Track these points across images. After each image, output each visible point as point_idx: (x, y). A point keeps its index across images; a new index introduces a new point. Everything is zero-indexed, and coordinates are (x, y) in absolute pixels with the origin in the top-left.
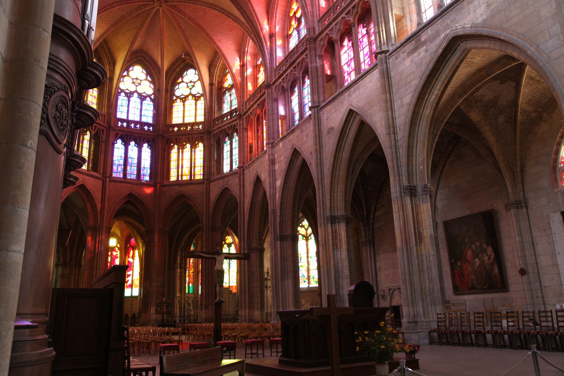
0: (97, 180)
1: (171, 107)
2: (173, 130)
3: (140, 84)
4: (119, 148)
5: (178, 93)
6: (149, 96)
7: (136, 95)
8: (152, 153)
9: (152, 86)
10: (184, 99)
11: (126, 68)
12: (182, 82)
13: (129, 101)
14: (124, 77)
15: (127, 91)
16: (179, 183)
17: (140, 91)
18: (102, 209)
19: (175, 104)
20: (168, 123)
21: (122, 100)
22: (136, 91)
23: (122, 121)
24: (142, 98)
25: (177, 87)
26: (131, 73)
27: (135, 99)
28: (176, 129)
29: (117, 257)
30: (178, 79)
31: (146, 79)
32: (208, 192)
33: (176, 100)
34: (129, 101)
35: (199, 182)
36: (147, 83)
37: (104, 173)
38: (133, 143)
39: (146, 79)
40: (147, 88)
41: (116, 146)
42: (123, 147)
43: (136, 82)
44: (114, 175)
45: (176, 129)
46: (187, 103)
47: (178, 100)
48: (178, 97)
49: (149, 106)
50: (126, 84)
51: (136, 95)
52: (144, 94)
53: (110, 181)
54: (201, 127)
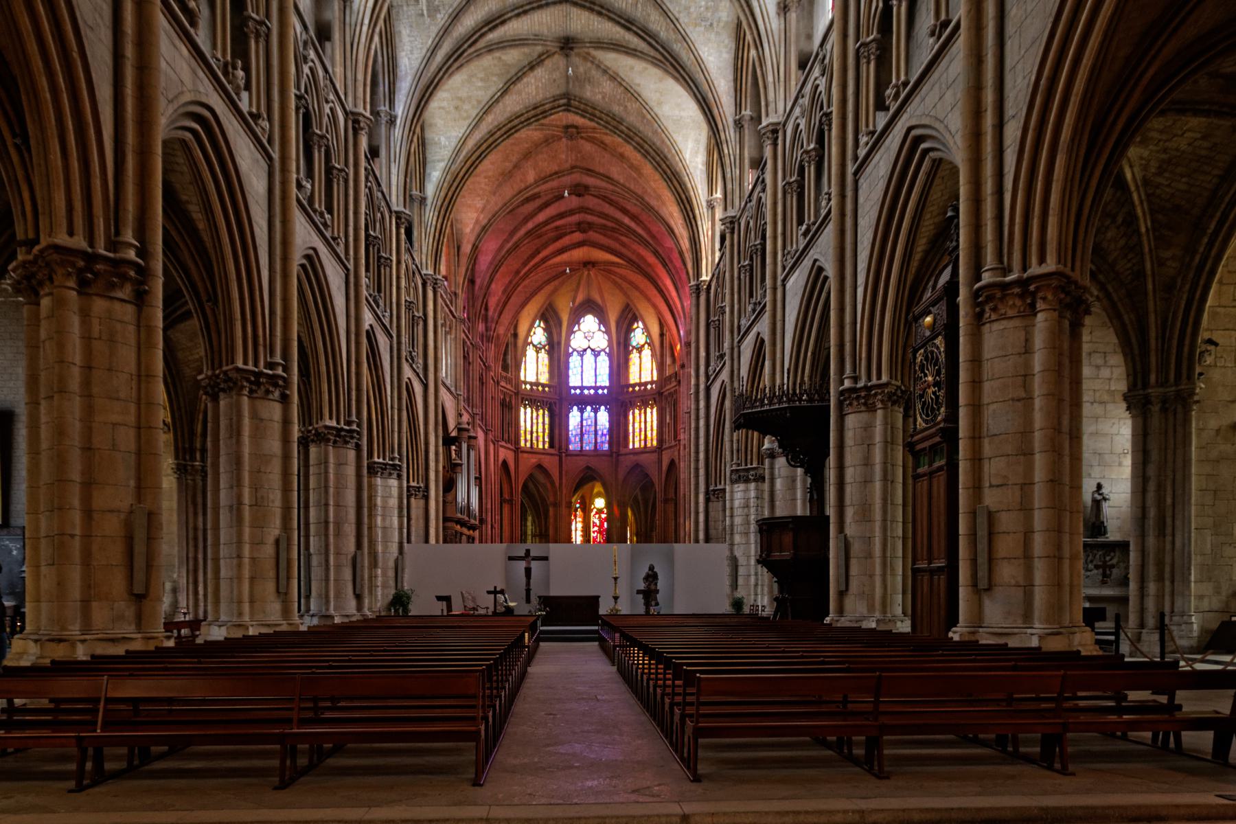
0: (553, 457)
1: (627, 361)
2: (628, 392)
3: (592, 337)
4: (574, 417)
5: (634, 343)
6: (604, 350)
7: (589, 351)
8: (610, 416)
9: (606, 337)
10: (640, 349)
11: (576, 319)
12: (638, 327)
13: (582, 360)
14: (574, 332)
15: (580, 349)
16: (635, 452)
17: (593, 347)
18: (561, 484)
19: (632, 356)
20: (623, 382)
21: (574, 361)
22: (589, 347)
23: (575, 388)
24: (596, 354)
25: (632, 335)
26: (582, 326)
27: (589, 356)
28: (631, 389)
30: (633, 324)
33: (632, 350)
34: (582, 360)
35: (653, 451)
37: (560, 448)
38: (589, 408)
39: (600, 330)
41: (571, 415)
42: (579, 414)
44: (571, 447)
45: (631, 389)
46: (644, 353)
47: (635, 351)
48: (634, 347)
49: (604, 361)
50: (577, 341)
51: (589, 351)
52: (598, 349)
53: (566, 456)
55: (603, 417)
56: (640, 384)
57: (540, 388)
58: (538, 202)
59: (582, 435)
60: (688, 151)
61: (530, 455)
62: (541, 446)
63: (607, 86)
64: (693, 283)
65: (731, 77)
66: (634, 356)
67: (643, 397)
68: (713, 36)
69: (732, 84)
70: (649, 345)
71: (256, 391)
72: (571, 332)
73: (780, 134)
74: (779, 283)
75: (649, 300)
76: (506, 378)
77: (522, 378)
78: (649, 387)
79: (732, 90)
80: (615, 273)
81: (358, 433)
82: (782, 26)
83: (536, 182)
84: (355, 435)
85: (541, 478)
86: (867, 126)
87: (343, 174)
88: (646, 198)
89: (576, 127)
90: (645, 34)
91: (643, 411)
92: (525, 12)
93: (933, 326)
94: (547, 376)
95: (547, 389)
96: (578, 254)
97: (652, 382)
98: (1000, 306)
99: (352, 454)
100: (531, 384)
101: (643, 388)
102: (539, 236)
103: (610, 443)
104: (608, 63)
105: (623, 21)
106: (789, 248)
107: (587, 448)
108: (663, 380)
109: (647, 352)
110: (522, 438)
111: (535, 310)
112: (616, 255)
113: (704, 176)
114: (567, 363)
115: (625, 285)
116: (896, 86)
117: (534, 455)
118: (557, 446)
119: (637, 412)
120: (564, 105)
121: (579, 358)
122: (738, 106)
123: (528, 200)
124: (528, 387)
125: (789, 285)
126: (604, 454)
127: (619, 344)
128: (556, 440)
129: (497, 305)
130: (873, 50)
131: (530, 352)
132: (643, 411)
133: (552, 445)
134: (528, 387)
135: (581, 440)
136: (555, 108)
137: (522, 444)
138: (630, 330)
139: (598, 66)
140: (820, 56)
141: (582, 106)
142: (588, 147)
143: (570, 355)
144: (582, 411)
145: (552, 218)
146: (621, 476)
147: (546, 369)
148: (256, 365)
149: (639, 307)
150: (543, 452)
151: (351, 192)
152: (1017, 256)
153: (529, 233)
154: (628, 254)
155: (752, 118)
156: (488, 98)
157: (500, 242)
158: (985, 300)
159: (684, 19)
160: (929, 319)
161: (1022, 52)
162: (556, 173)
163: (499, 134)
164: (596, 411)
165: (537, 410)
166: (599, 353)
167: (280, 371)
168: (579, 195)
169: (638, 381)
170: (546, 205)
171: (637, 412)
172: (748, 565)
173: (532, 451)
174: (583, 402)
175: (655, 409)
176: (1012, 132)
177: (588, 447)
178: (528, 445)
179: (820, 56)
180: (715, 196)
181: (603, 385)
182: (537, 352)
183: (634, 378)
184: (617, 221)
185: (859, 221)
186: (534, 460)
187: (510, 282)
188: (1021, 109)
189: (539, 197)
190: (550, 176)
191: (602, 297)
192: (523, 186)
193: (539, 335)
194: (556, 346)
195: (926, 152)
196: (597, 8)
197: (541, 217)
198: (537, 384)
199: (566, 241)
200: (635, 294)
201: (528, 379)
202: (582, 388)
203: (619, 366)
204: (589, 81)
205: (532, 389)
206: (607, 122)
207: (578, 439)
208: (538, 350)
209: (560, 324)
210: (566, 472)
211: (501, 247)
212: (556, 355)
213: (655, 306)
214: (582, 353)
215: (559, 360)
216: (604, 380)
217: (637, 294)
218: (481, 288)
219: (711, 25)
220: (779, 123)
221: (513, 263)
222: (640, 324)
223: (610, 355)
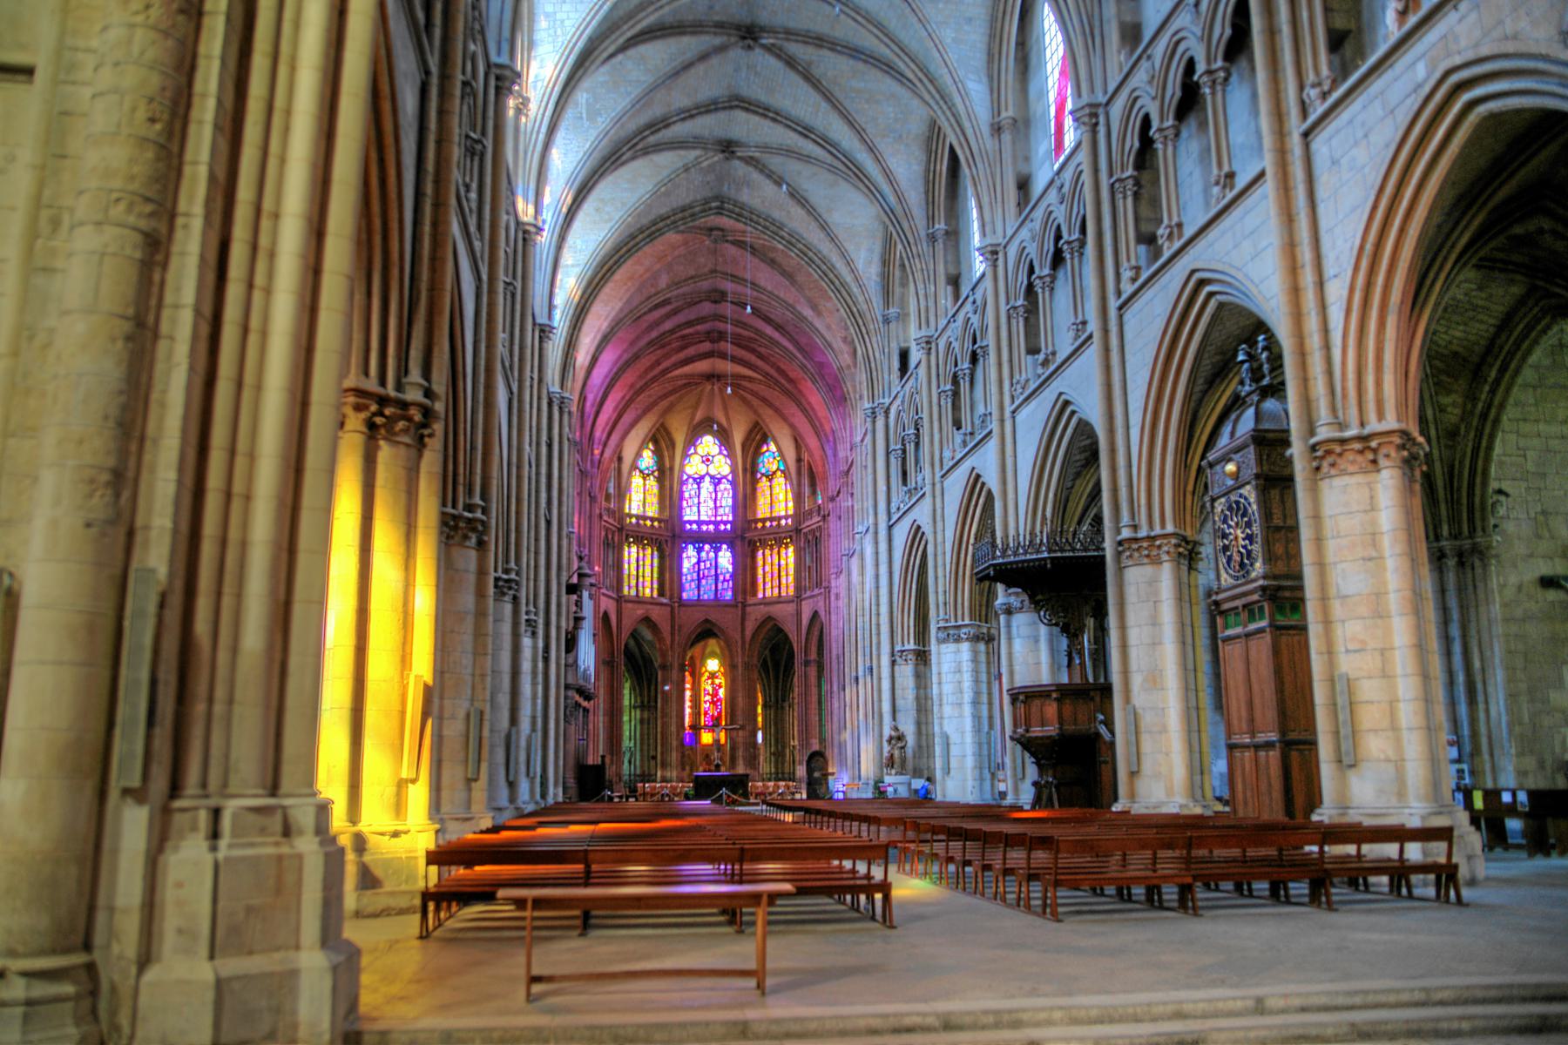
4: (690, 557)
6: (725, 477)
7: (707, 479)
8: (734, 556)
10: (770, 477)
11: (692, 441)
13: (699, 488)
16: (766, 602)
17: (713, 472)
19: (760, 485)
22: (708, 474)
23: (691, 523)
24: (716, 481)
27: (707, 485)
29: (720, 686)
30: (761, 447)
31: (721, 453)
32: (799, 613)
36: (722, 458)
38: (707, 547)
39: (721, 453)
40: (722, 466)
43: (707, 460)
44: (685, 596)
46: (776, 482)
48: (763, 474)
50: (694, 466)
51: (707, 479)
54: (789, 521)
55: (725, 559)
56: (771, 519)
57: (648, 523)
58: (668, 308)
59: (699, 580)
60: (861, 261)
61: (636, 606)
62: (648, 591)
63: (768, 188)
64: (867, 405)
65: (922, 189)
66: (764, 483)
67: (777, 537)
68: (902, 147)
69: (923, 196)
70: (782, 471)
71: (453, 537)
72: (686, 455)
73: (1001, 255)
74: (1007, 414)
75: (785, 419)
76: (608, 509)
77: (627, 511)
78: (783, 522)
79: (923, 203)
80: (745, 389)
81: (517, 583)
82: (997, 147)
83: (668, 287)
84: (513, 585)
85: (647, 634)
86: (1128, 259)
87: (511, 288)
88: (799, 308)
89: (722, 230)
90: (825, 142)
91: (776, 551)
92: (692, 116)
93: (1236, 476)
94: (656, 507)
95: (656, 524)
96: (702, 366)
97: (786, 517)
98: (1339, 461)
99: (508, 608)
100: (638, 517)
101: (775, 523)
102: (663, 346)
103: (734, 589)
104: (773, 168)
105: (800, 129)
106: (1017, 377)
107: (706, 597)
108: (800, 515)
109: (780, 481)
110: (626, 584)
111: (646, 430)
112: (750, 368)
113: (879, 288)
114: (682, 493)
115: (755, 402)
116: (1169, 226)
117: (640, 606)
118: (668, 593)
119: (768, 552)
120: (717, 208)
121: (695, 486)
122: (931, 219)
123: (656, 307)
124: (634, 520)
125: (1020, 417)
126: (728, 605)
127: (745, 470)
128: (667, 587)
129: (607, 424)
130: (1129, 187)
131: (637, 480)
132: (776, 551)
133: (661, 593)
134: (634, 520)
135: (699, 588)
136: (704, 211)
137: (626, 591)
138: (757, 453)
139: (762, 171)
140: (1058, 183)
141: (737, 210)
142: (733, 250)
143: (683, 483)
144: (699, 550)
145: (679, 326)
146: (749, 633)
147: (655, 500)
148: (454, 506)
149: (771, 426)
150: (651, 602)
151: (518, 307)
152: (1353, 412)
153: (650, 343)
154: (767, 368)
155: (947, 233)
156: (633, 200)
157: (619, 352)
158: (1323, 454)
159: (870, 129)
160: (1231, 467)
161: (1341, 217)
162: (692, 278)
163: (640, 237)
164: (717, 550)
165: (644, 549)
166: (720, 481)
167: (479, 515)
168: (715, 302)
169: (768, 515)
170: (675, 312)
171: (768, 552)
172: (963, 743)
173: (638, 600)
174: (699, 539)
175: (791, 549)
176: (1336, 292)
177: (707, 595)
178: (633, 592)
179: (1058, 183)
180: (891, 310)
181: (725, 518)
182: (644, 479)
183: (763, 510)
184: (757, 331)
185: (1128, 356)
186: (640, 611)
187: (623, 398)
188: (1346, 270)
189: (670, 303)
190: (686, 280)
191: (728, 419)
192: (653, 291)
193: (647, 460)
194: (668, 473)
195: (1211, 295)
196: (771, 115)
197: (668, 325)
198: (645, 518)
199: (691, 351)
200: (767, 413)
201: (634, 512)
202: (700, 523)
203: (745, 496)
204: (748, 185)
205: (638, 523)
206: (764, 227)
207: (694, 585)
208: (645, 477)
209: (673, 445)
210: (680, 626)
211: (620, 357)
212: (667, 483)
213: (792, 426)
214: (699, 480)
215: (671, 488)
216: (726, 513)
217: (770, 412)
218: (593, 405)
219: (900, 136)
220: (999, 245)
221: (629, 377)
222: (773, 447)
223: (733, 483)
